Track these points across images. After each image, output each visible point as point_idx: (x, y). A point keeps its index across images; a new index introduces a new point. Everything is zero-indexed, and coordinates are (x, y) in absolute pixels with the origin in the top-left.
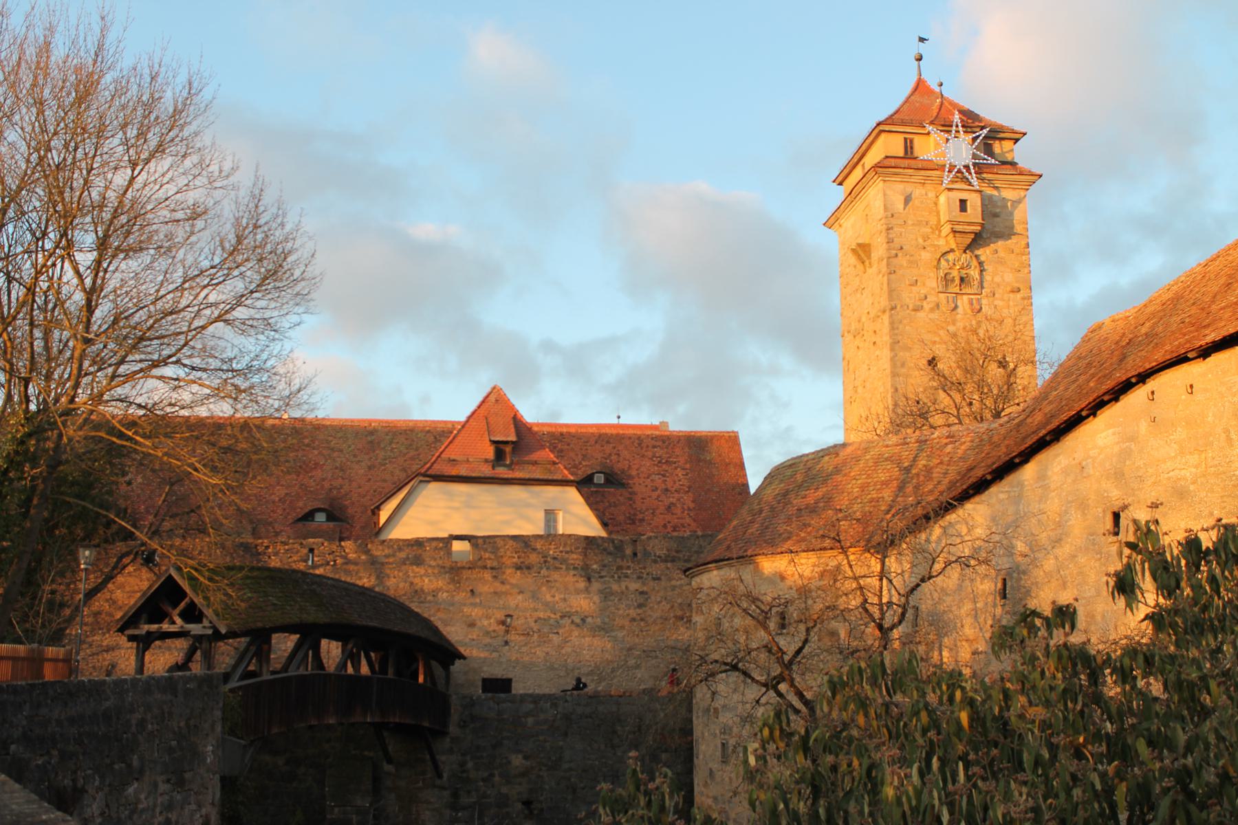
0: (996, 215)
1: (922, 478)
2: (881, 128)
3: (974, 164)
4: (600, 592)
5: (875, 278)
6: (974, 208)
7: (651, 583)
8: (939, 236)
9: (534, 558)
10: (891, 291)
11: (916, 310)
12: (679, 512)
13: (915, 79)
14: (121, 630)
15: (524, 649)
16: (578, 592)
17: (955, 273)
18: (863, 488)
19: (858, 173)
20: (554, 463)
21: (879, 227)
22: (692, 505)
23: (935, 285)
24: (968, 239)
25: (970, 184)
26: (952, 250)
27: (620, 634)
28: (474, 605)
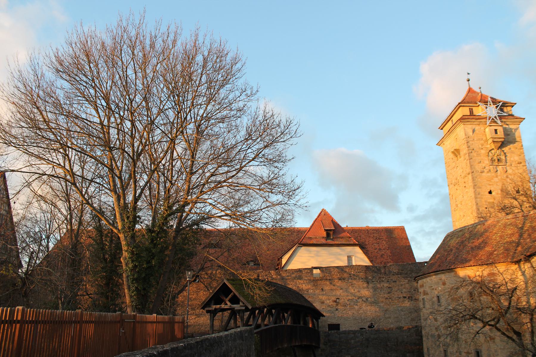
0: (508, 135)
1: (530, 231)
2: (460, 105)
3: (493, 119)
4: (373, 287)
5: (463, 162)
6: (500, 132)
7: (393, 284)
8: (487, 144)
9: (346, 275)
10: (471, 166)
11: (482, 172)
12: (386, 257)
13: (468, 88)
14: (203, 308)
15: (344, 312)
16: (364, 288)
17: (495, 158)
18: (501, 237)
19: (450, 124)
20: (350, 237)
21: (463, 142)
22: (390, 254)
23: (488, 162)
24: (499, 144)
25: (497, 123)
26: (493, 149)
27: (382, 305)
28: (323, 295)
